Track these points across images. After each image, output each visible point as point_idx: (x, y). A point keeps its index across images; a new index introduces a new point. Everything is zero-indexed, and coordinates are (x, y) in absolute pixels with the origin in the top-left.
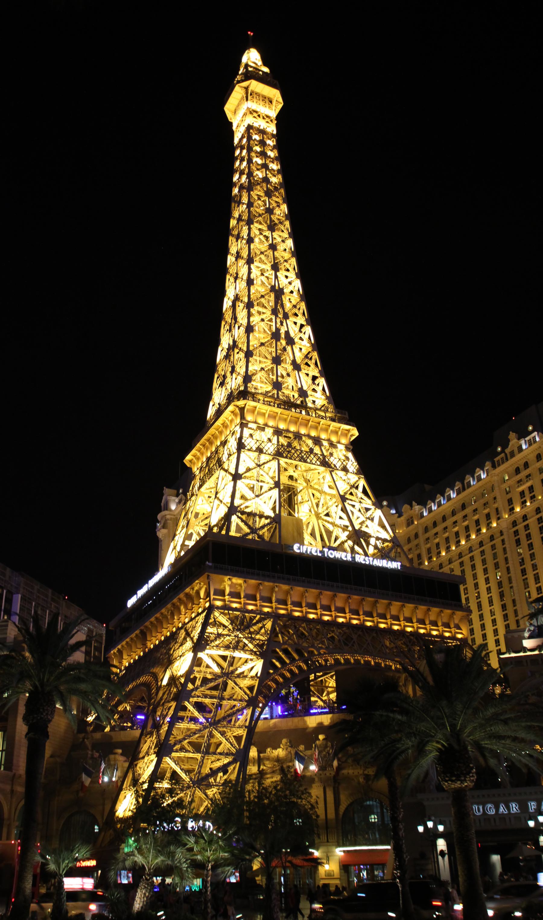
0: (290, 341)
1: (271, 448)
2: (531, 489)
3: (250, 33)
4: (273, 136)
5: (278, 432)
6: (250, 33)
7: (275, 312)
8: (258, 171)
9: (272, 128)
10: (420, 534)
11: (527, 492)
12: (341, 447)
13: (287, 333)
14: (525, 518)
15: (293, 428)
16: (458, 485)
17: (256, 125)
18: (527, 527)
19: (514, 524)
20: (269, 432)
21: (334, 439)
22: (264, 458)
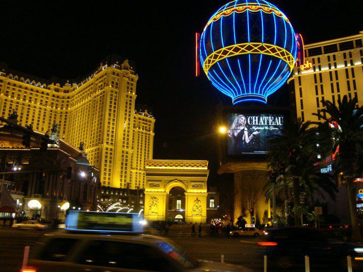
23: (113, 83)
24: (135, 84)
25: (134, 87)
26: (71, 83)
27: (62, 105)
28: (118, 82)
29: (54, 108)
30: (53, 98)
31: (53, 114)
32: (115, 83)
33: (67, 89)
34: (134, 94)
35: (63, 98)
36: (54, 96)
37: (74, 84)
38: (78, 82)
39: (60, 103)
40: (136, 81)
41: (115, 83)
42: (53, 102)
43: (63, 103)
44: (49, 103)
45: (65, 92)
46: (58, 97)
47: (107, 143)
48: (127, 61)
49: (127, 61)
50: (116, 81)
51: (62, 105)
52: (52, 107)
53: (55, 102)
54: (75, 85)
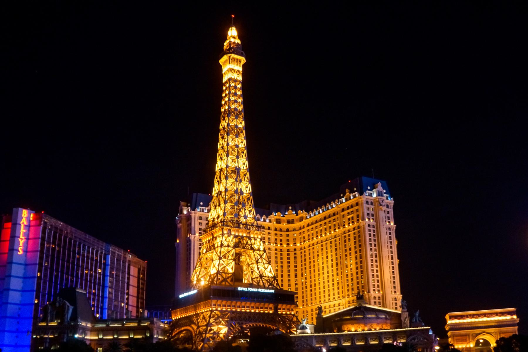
0: (242, 193)
1: (232, 244)
2: (352, 218)
3: (233, 16)
4: (240, 82)
5: (235, 237)
6: (233, 16)
7: (236, 180)
8: (233, 100)
9: (240, 78)
10: (305, 227)
11: (351, 219)
12: (258, 240)
13: (241, 189)
14: (349, 231)
15: (241, 234)
16: (323, 207)
17: (233, 77)
18: (349, 235)
19: (345, 233)
20: (232, 237)
21: (256, 237)
22: (230, 249)
23: (368, 214)
24: (391, 210)
25: (391, 215)
26: (295, 209)
27: (288, 240)
28: (373, 213)
29: (279, 245)
30: (276, 232)
31: (279, 253)
32: (370, 215)
33: (291, 219)
34: (392, 224)
35: (288, 230)
36: (276, 229)
37: (300, 212)
38: (309, 209)
39: (284, 238)
40: (392, 207)
41: (370, 215)
42: (276, 237)
43: (288, 238)
44: (273, 240)
45: (289, 222)
46: (281, 230)
47: (374, 290)
48: (380, 184)
49: (380, 184)
50: (371, 212)
51: (288, 240)
52: (276, 243)
53: (279, 238)
54: (302, 213)
